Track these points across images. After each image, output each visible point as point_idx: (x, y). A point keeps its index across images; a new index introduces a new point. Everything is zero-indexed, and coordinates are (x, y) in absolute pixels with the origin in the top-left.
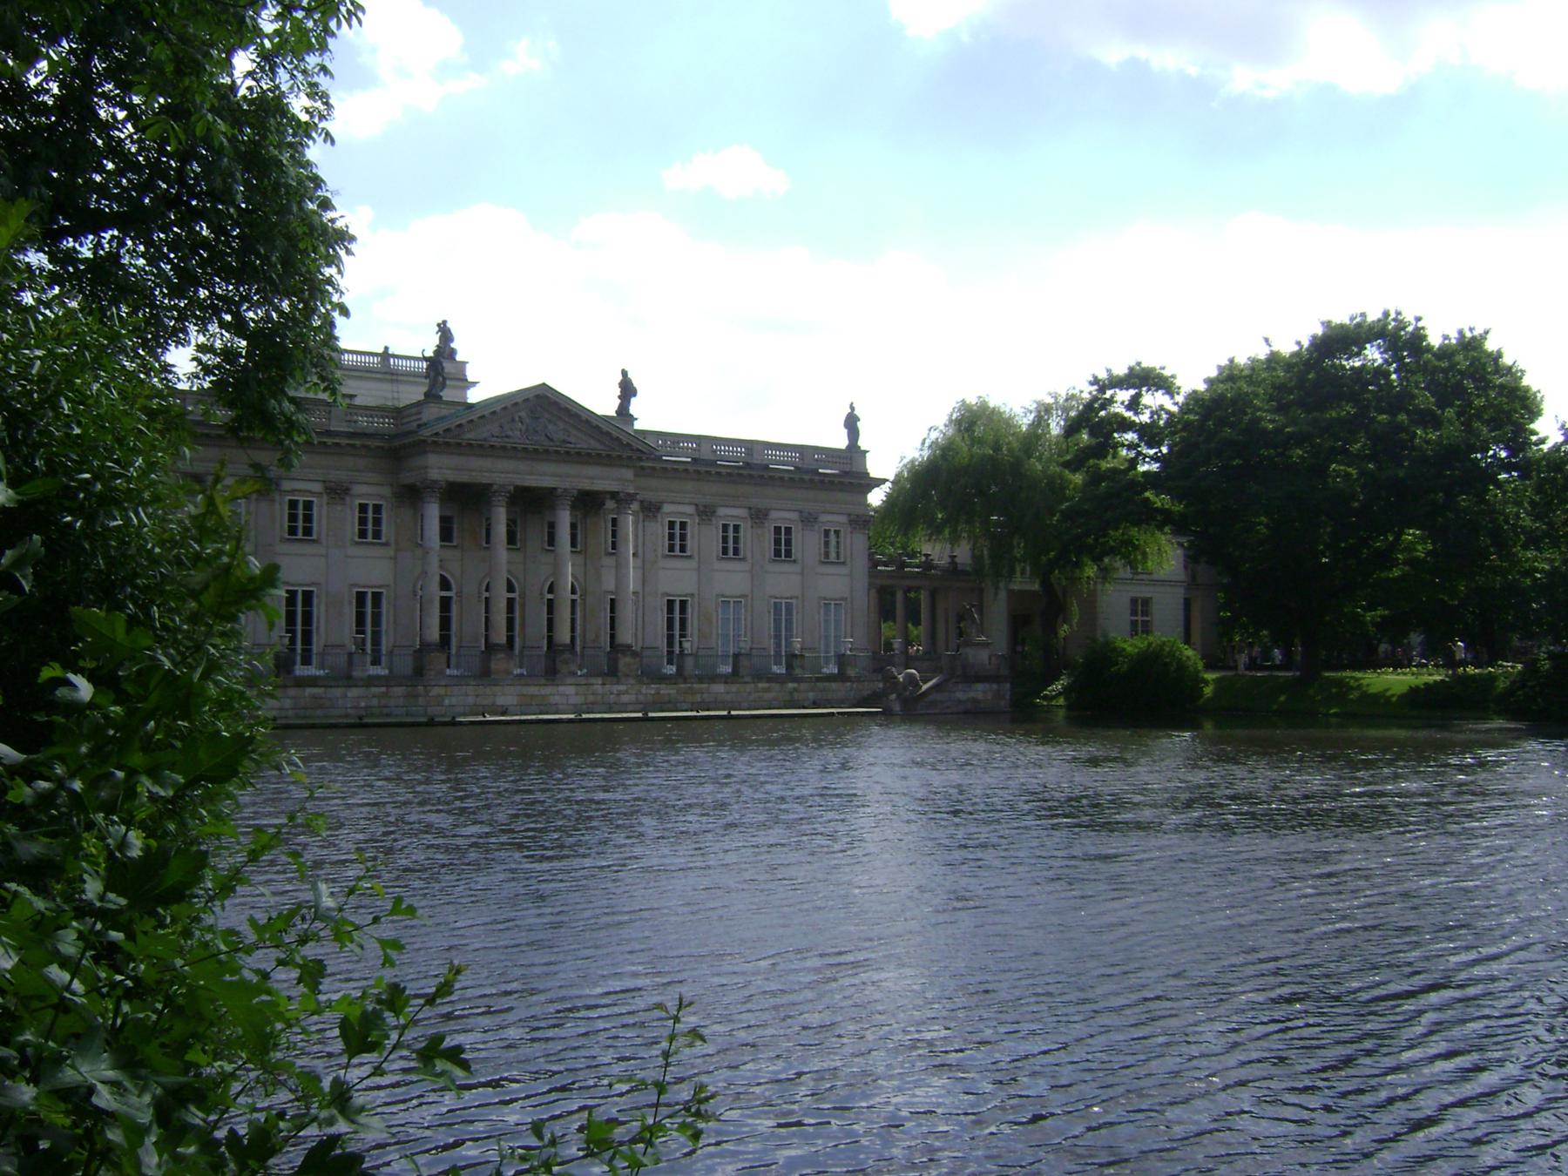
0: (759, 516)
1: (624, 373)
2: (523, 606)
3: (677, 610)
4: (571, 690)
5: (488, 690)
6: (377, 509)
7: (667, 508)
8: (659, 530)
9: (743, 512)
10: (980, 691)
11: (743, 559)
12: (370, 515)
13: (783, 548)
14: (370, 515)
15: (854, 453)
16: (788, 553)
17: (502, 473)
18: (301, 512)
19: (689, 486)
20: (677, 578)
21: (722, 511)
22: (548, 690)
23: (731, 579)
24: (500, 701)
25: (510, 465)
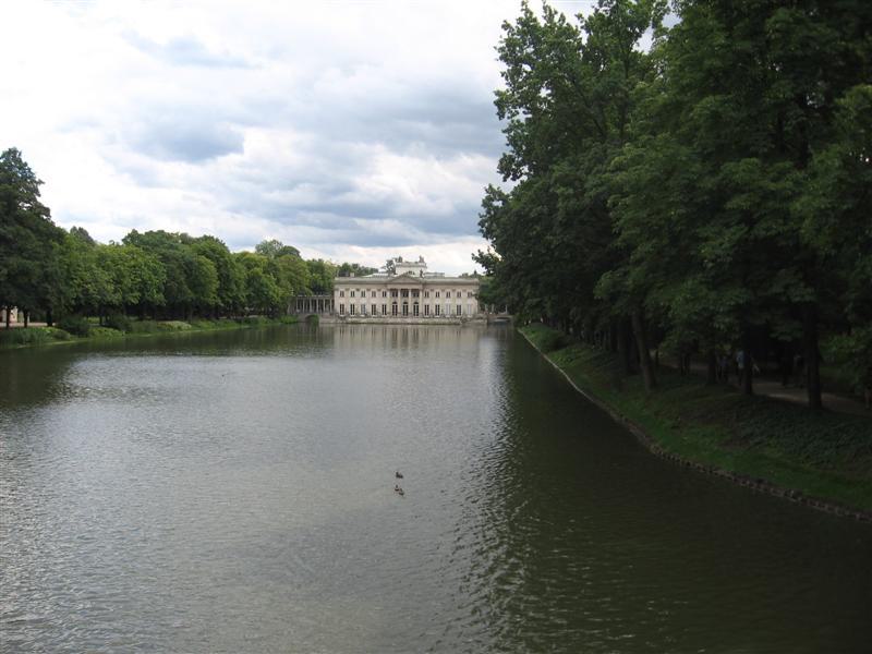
3: (437, 307)
10: (480, 321)
13: (459, 295)
17: (399, 287)
20: (437, 301)
23: (448, 301)
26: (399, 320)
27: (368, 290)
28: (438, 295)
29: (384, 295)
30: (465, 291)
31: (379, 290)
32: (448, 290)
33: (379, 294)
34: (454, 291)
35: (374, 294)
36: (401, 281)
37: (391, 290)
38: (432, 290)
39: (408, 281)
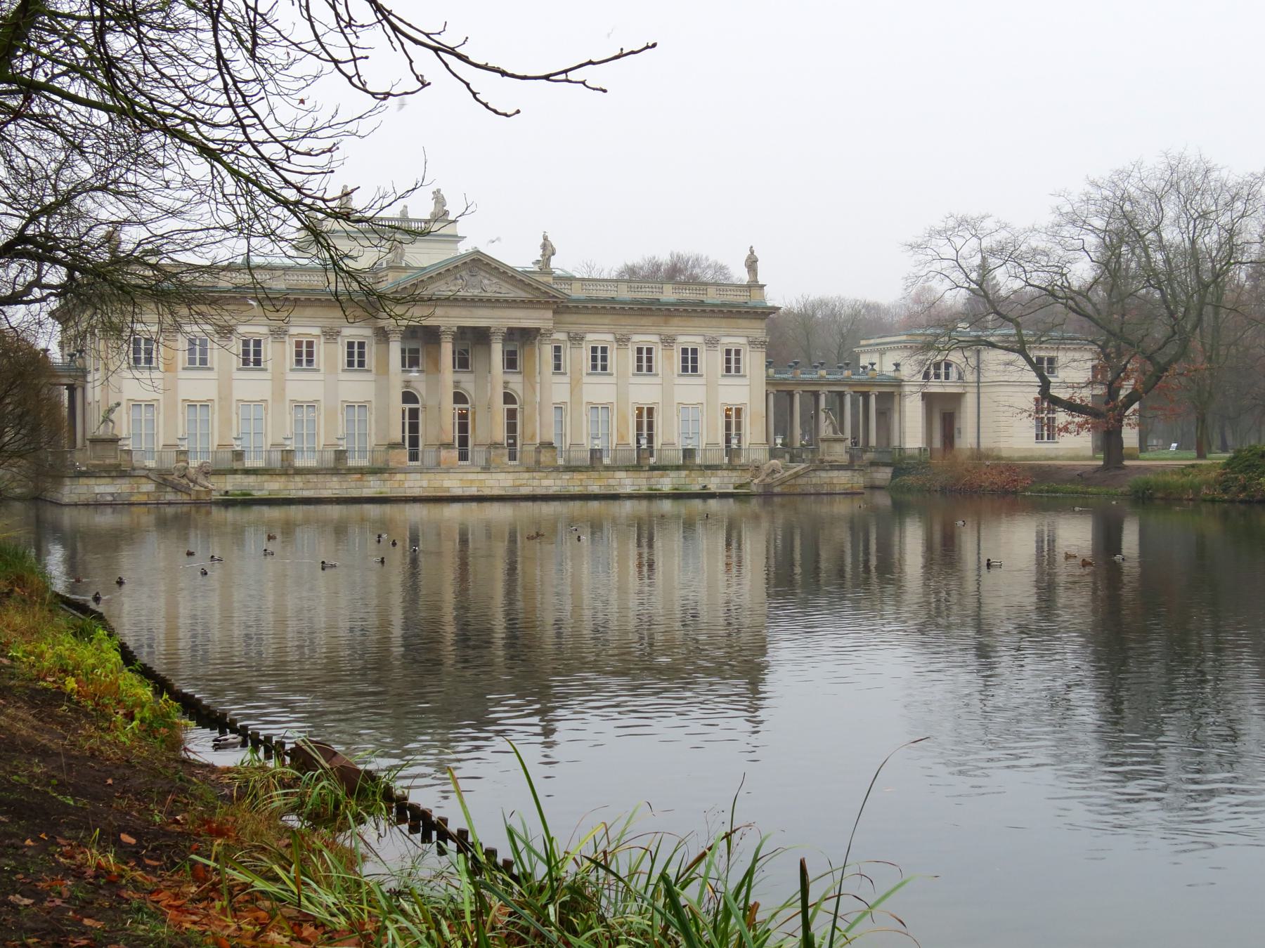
0: (668, 341)
1: (545, 239)
2: (474, 413)
4: (502, 476)
5: (438, 476)
6: (361, 345)
7: (589, 337)
8: (586, 354)
9: (655, 338)
11: (656, 375)
12: (356, 350)
13: (690, 362)
14: (356, 350)
15: (755, 286)
16: (695, 369)
17: (449, 319)
18: (304, 349)
19: (607, 319)
21: (636, 338)
22: (482, 476)
24: (447, 484)
25: (455, 311)
26: (453, 484)
27: (279, 334)
28: (599, 360)
29: (356, 357)
30: (712, 343)
31: (331, 335)
32: (641, 339)
33: (331, 355)
34: (668, 341)
35: (305, 356)
36: (443, 289)
37: (411, 333)
38: (576, 339)
39: (492, 287)
